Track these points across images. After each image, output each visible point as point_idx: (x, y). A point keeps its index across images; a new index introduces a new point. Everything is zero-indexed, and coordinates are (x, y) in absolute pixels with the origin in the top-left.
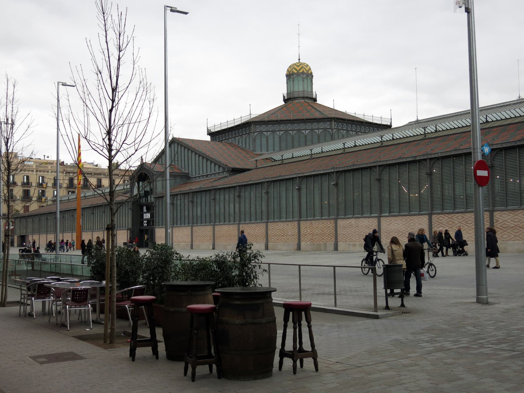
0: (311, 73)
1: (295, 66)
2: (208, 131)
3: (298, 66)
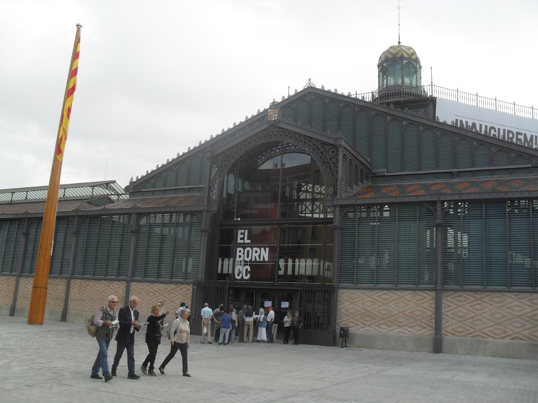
0: (417, 60)
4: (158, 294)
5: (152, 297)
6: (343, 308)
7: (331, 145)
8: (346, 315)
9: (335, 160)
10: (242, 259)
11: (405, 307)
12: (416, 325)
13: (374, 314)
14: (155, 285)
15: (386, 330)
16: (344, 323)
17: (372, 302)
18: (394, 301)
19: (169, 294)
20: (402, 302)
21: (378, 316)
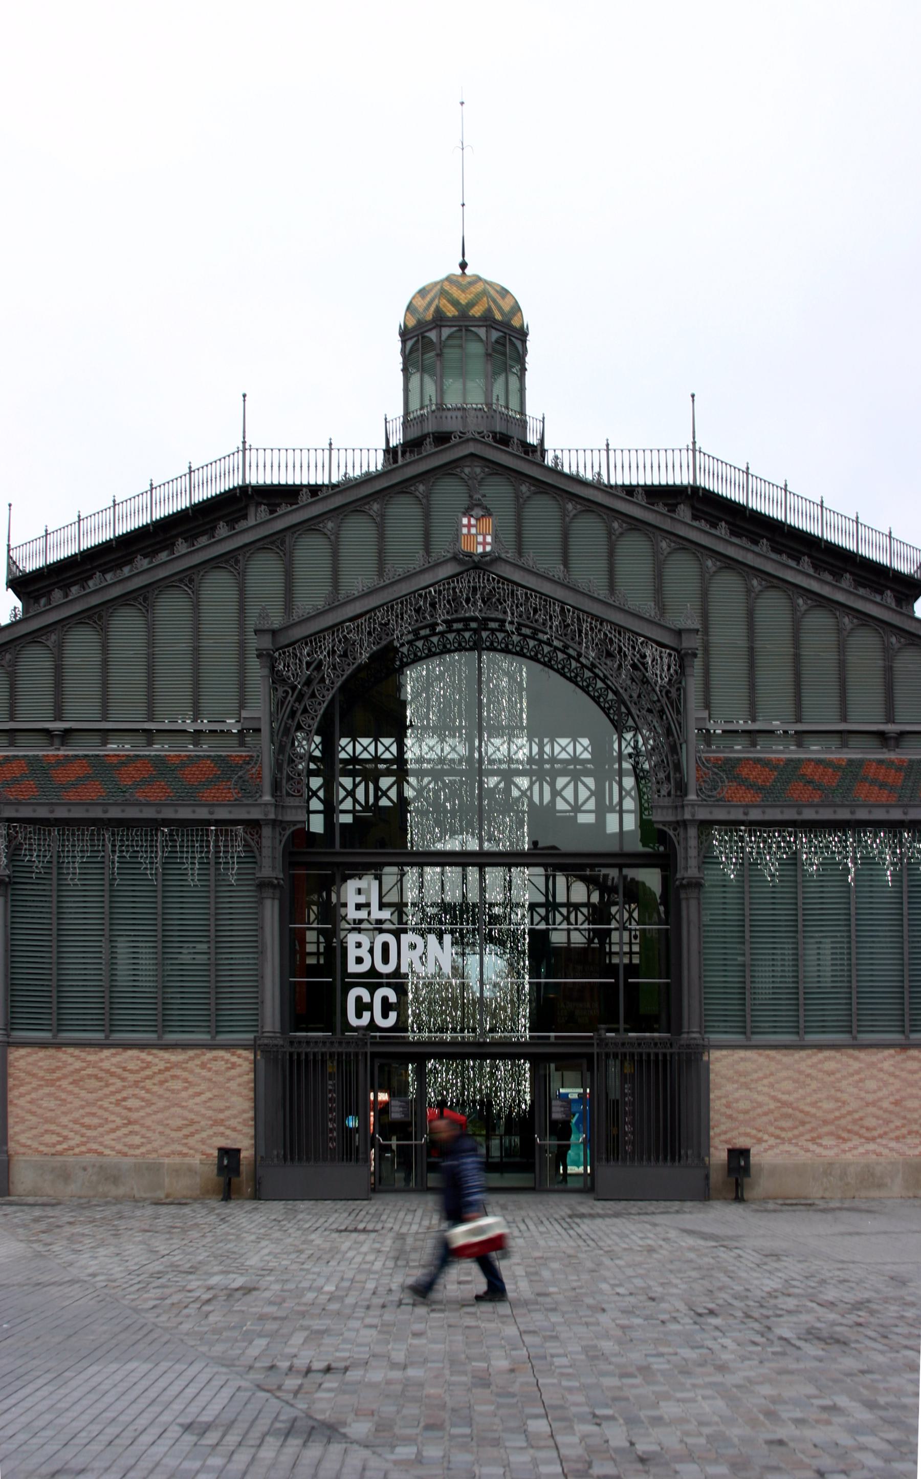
0: (522, 334)
1: (447, 287)
3: (463, 289)
4: (119, 1084)
5: (100, 1094)
6: (719, 1098)
8: (730, 1117)
10: (364, 967)
11: (880, 1089)
12: (910, 1133)
13: (802, 1111)
14: (106, 1053)
15: (836, 1150)
16: (723, 1137)
17: (795, 1081)
18: (852, 1075)
19: (161, 1083)
20: (872, 1077)
21: (814, 1116)
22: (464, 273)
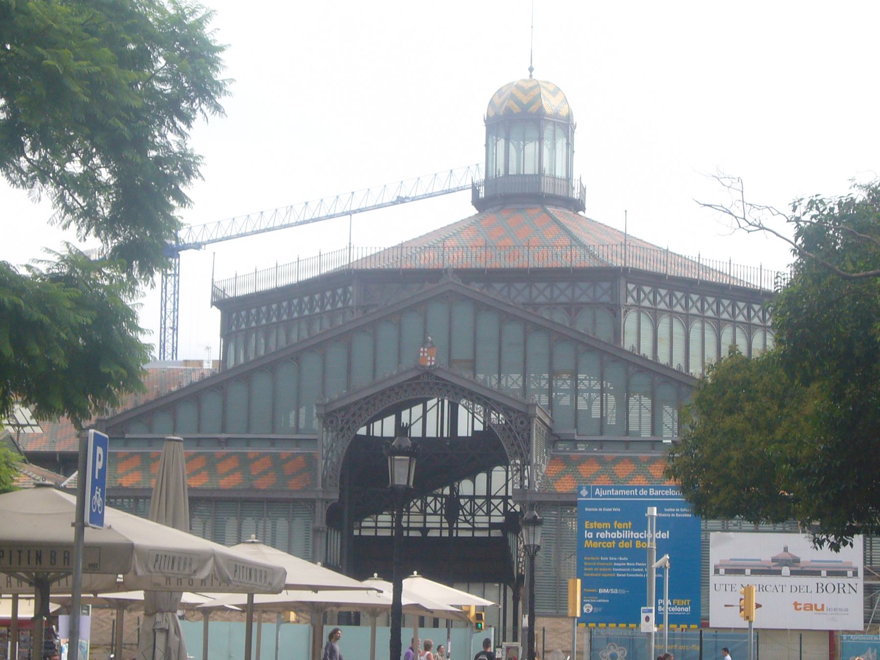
2: (214, 294)
7: (519, 412)
9: (525, 436)
22: (531, 76)
